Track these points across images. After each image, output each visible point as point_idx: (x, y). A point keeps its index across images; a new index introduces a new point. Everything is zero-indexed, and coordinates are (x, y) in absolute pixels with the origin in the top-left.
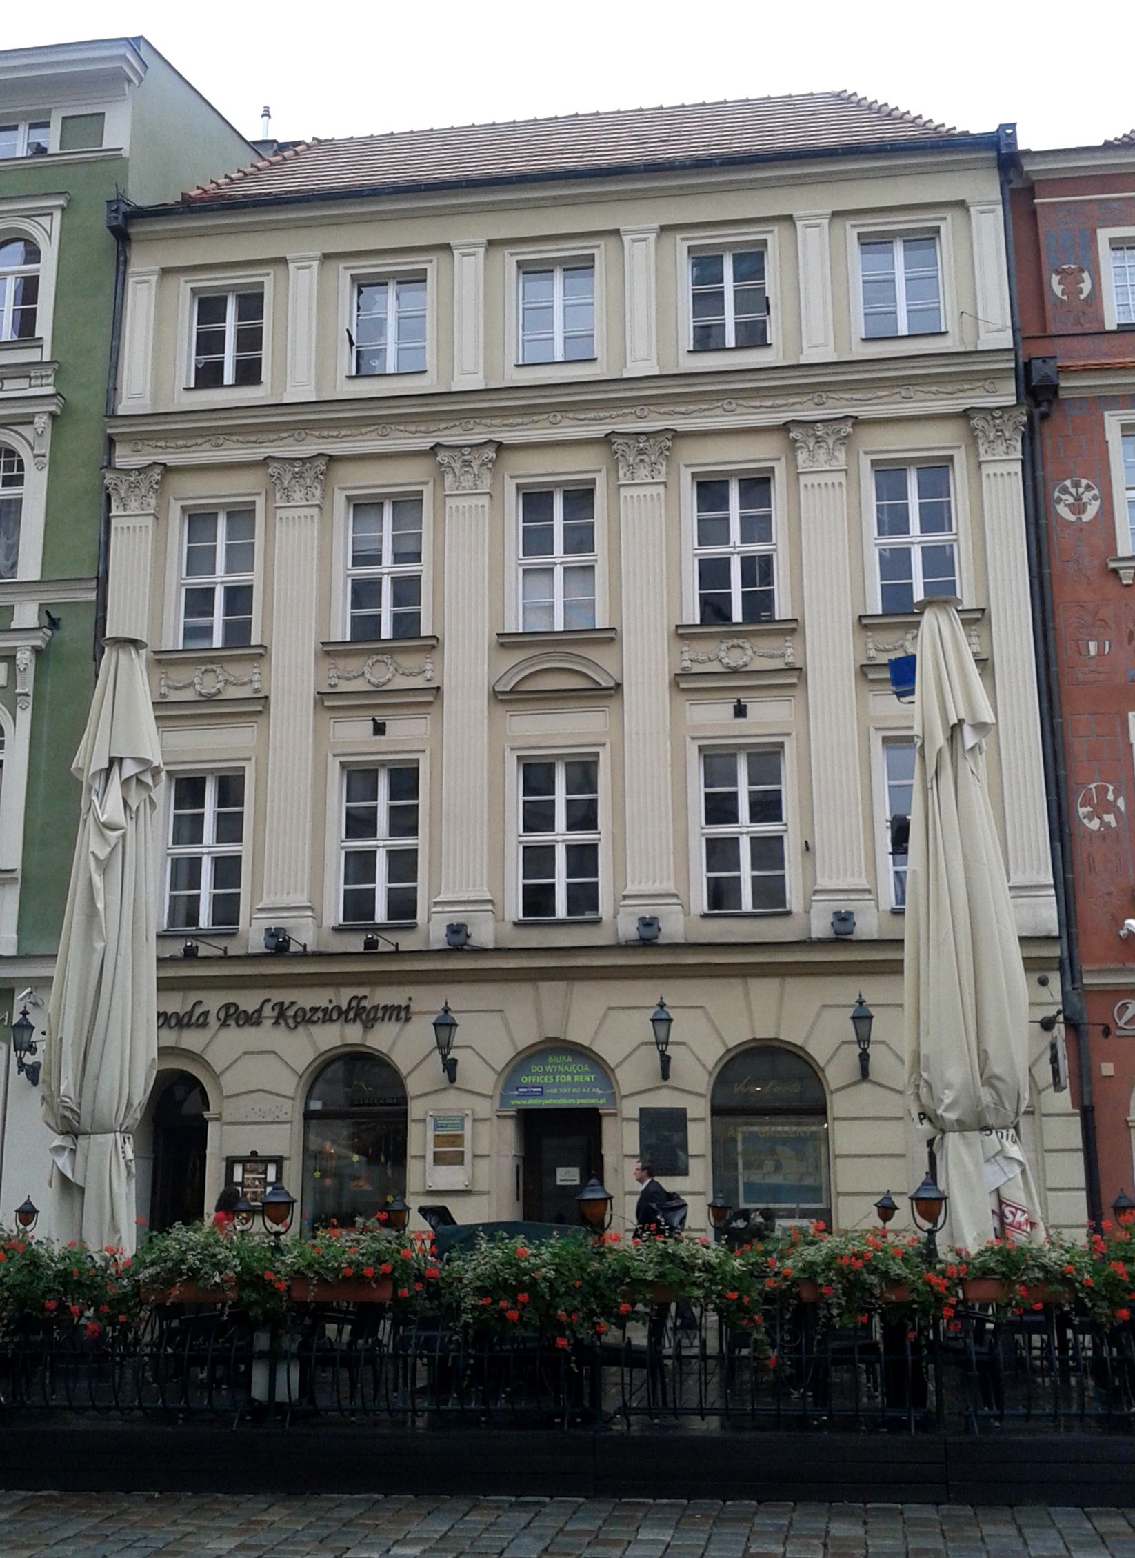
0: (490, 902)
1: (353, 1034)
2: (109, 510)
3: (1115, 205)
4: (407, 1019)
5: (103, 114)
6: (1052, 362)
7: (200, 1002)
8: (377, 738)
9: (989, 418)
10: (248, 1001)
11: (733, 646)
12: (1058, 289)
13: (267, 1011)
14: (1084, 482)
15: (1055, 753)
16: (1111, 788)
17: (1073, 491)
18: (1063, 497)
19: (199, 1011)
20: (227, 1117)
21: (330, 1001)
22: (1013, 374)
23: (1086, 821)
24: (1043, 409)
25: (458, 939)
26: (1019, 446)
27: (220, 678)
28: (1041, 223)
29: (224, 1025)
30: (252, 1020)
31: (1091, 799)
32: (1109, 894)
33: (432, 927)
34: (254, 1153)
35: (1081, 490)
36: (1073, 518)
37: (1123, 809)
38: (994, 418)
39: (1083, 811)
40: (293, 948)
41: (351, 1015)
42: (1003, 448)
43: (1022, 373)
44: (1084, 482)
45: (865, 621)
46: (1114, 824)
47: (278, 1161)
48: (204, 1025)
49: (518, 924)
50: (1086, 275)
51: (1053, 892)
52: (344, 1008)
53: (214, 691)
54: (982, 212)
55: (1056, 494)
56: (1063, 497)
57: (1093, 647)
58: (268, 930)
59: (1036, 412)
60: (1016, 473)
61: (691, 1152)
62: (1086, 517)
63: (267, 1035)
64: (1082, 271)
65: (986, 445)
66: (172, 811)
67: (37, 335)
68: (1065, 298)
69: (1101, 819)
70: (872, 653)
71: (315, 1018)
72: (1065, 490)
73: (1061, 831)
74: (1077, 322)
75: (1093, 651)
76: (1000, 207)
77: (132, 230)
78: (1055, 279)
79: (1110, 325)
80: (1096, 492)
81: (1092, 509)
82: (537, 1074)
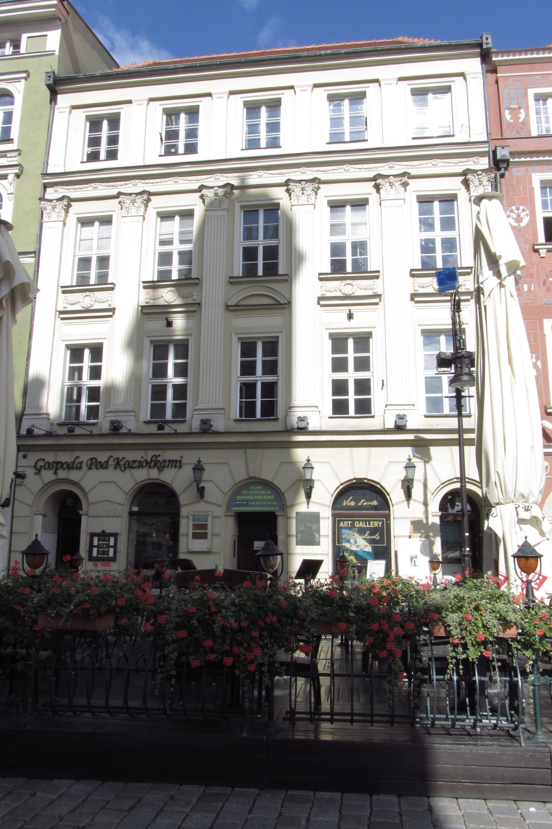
0: (223, 409)
1: (154, 474)
2: (42, 219)
3: (537, 77)
4: (180, 467)
5: (46, 36)
6: (507, 148)
7: (78, 457)
8: (168, 328)
10: (102, 457)
11: (348, 284)
13: (111, 462)
14: (521, 207)
17: (516, 212)
19: (78, 461)
20: (90, 514)
21: (142, 458)
24: (502, 171)
25: (206, 427)
27: (93, 299)
29: (90, 468)
30: (103, 466)
33: (194, 421)
34: (103, 531)
35: (520, 211)
38: (478, 175)
40: (123, 431)
41: (152, 464)
44: (521, 207)
45: (413, 273)
47: (115, 535)
48: (80, 468)
49: (236, 421)
50: (522, 111)
52: (149, 461)
53: (90, 305)
54: (473, 78)
56: (512, 215)
58: (111, 421)
59: (498, 173)
61: (321, 533)
62: (523, 224)
63: (111, 474)
64: (520, 108)
65: (474, 188)
66: (68, 365)
67: (11, 138)
68: (512, 121)
70: (417, 288)
71: (134, 466)
74: (518, 132)
76: (481, 76)
77: (58, 88)
78: (507, 112)
80: (527, 212)
81: (525, 221)
82: (245, 495)
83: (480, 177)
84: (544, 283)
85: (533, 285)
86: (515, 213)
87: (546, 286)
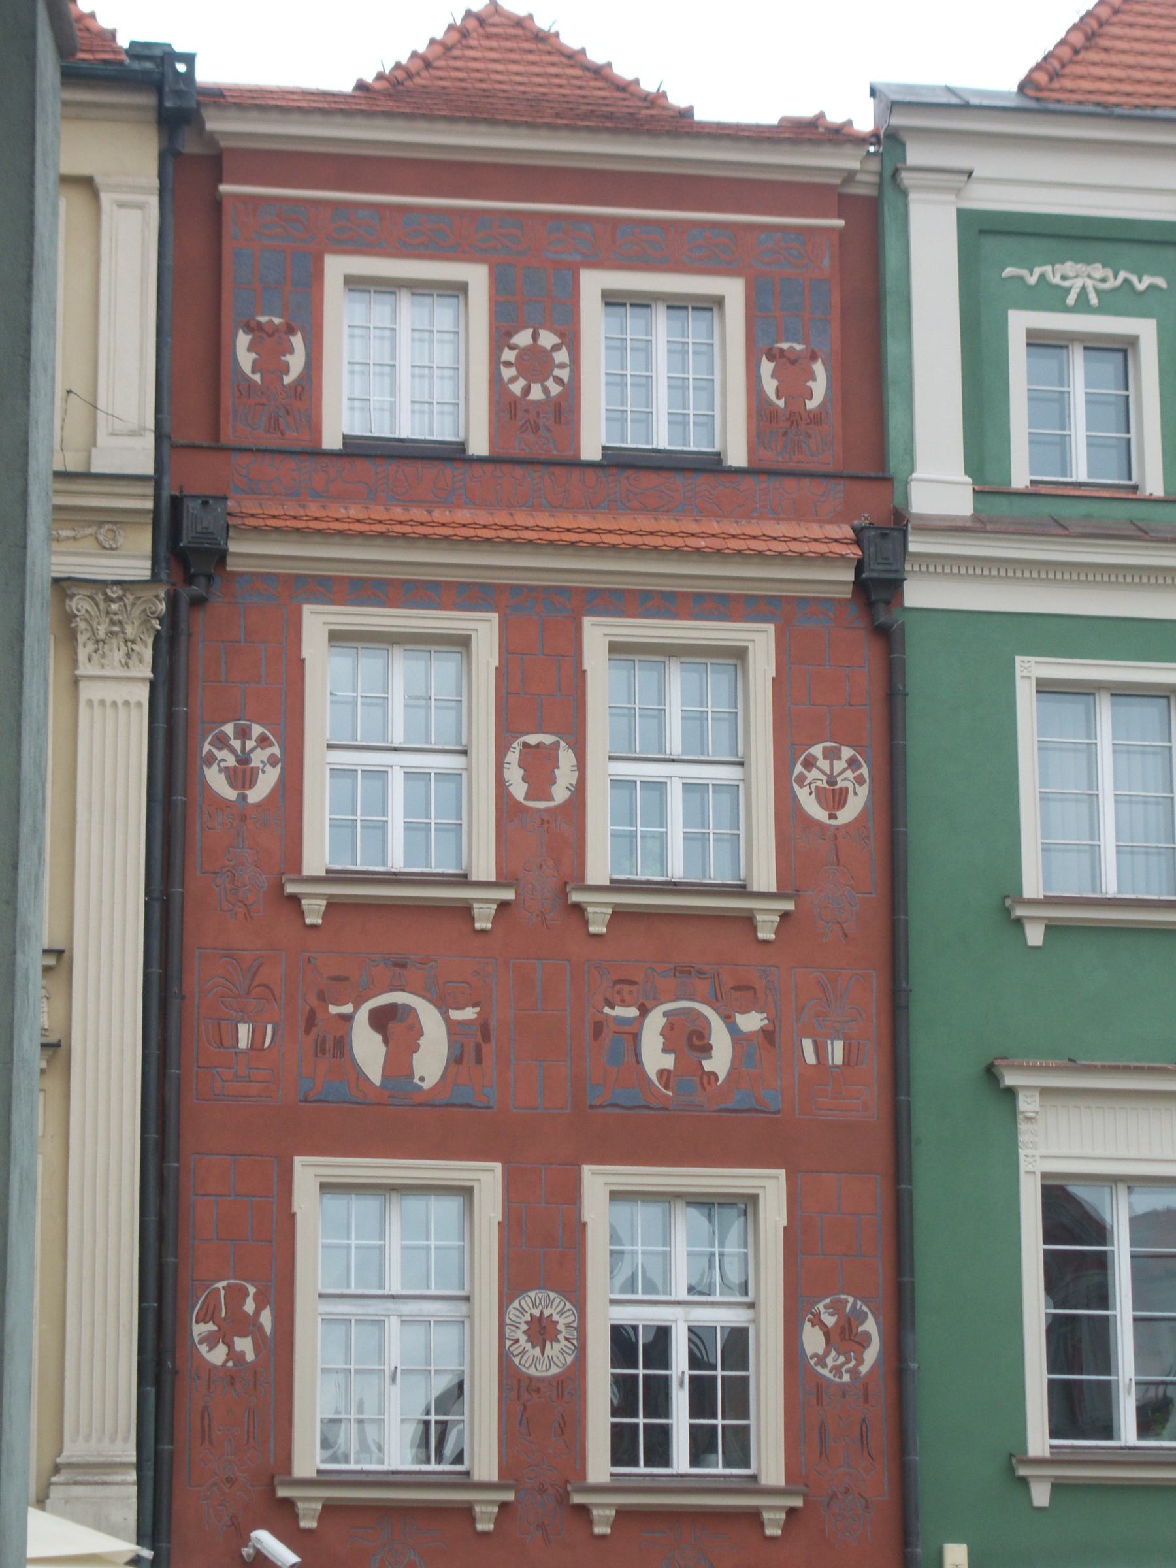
9: (100, 597)
12: (245, 359)
14: (257, 730)
15: (161, 1224)
16: (252, 1290)
17: (236, 744)
18: (220, 755)
22: (149, 519)
23: (203, 1349)
26: (148, 654)
28: (231, 228)
31: (217, 1308)
32: (230, 1481)
35: (250, 744)
36: (231, 794)
37: (268, 1327)
39: (200, 1329)
42: (119, 656)
44: (257, 730)
46: (250, 1356)
50: (297, 341)
51: (132, 1476)
54: (122, 205)
55: (207, 748)
56: (220, 755)
57: (244, 1031)
59: (185, 593)
60: (139, 704)
62: (256, 795)
64: (291, 330)
65: (91, 647)
68: (257, 378)
69: (230, 1346)
72: (222, 742)
73: (159, 1363)
74: (274, 425)
75: (243, 1044)
76: (154, 201)
78: (243, 340)
79: (331, 441)
81: (267, 782)
83: (114, 607)
84: (311, 1020)
85: (270, 1027)
86: (232, 751)
87: (315, 1031)
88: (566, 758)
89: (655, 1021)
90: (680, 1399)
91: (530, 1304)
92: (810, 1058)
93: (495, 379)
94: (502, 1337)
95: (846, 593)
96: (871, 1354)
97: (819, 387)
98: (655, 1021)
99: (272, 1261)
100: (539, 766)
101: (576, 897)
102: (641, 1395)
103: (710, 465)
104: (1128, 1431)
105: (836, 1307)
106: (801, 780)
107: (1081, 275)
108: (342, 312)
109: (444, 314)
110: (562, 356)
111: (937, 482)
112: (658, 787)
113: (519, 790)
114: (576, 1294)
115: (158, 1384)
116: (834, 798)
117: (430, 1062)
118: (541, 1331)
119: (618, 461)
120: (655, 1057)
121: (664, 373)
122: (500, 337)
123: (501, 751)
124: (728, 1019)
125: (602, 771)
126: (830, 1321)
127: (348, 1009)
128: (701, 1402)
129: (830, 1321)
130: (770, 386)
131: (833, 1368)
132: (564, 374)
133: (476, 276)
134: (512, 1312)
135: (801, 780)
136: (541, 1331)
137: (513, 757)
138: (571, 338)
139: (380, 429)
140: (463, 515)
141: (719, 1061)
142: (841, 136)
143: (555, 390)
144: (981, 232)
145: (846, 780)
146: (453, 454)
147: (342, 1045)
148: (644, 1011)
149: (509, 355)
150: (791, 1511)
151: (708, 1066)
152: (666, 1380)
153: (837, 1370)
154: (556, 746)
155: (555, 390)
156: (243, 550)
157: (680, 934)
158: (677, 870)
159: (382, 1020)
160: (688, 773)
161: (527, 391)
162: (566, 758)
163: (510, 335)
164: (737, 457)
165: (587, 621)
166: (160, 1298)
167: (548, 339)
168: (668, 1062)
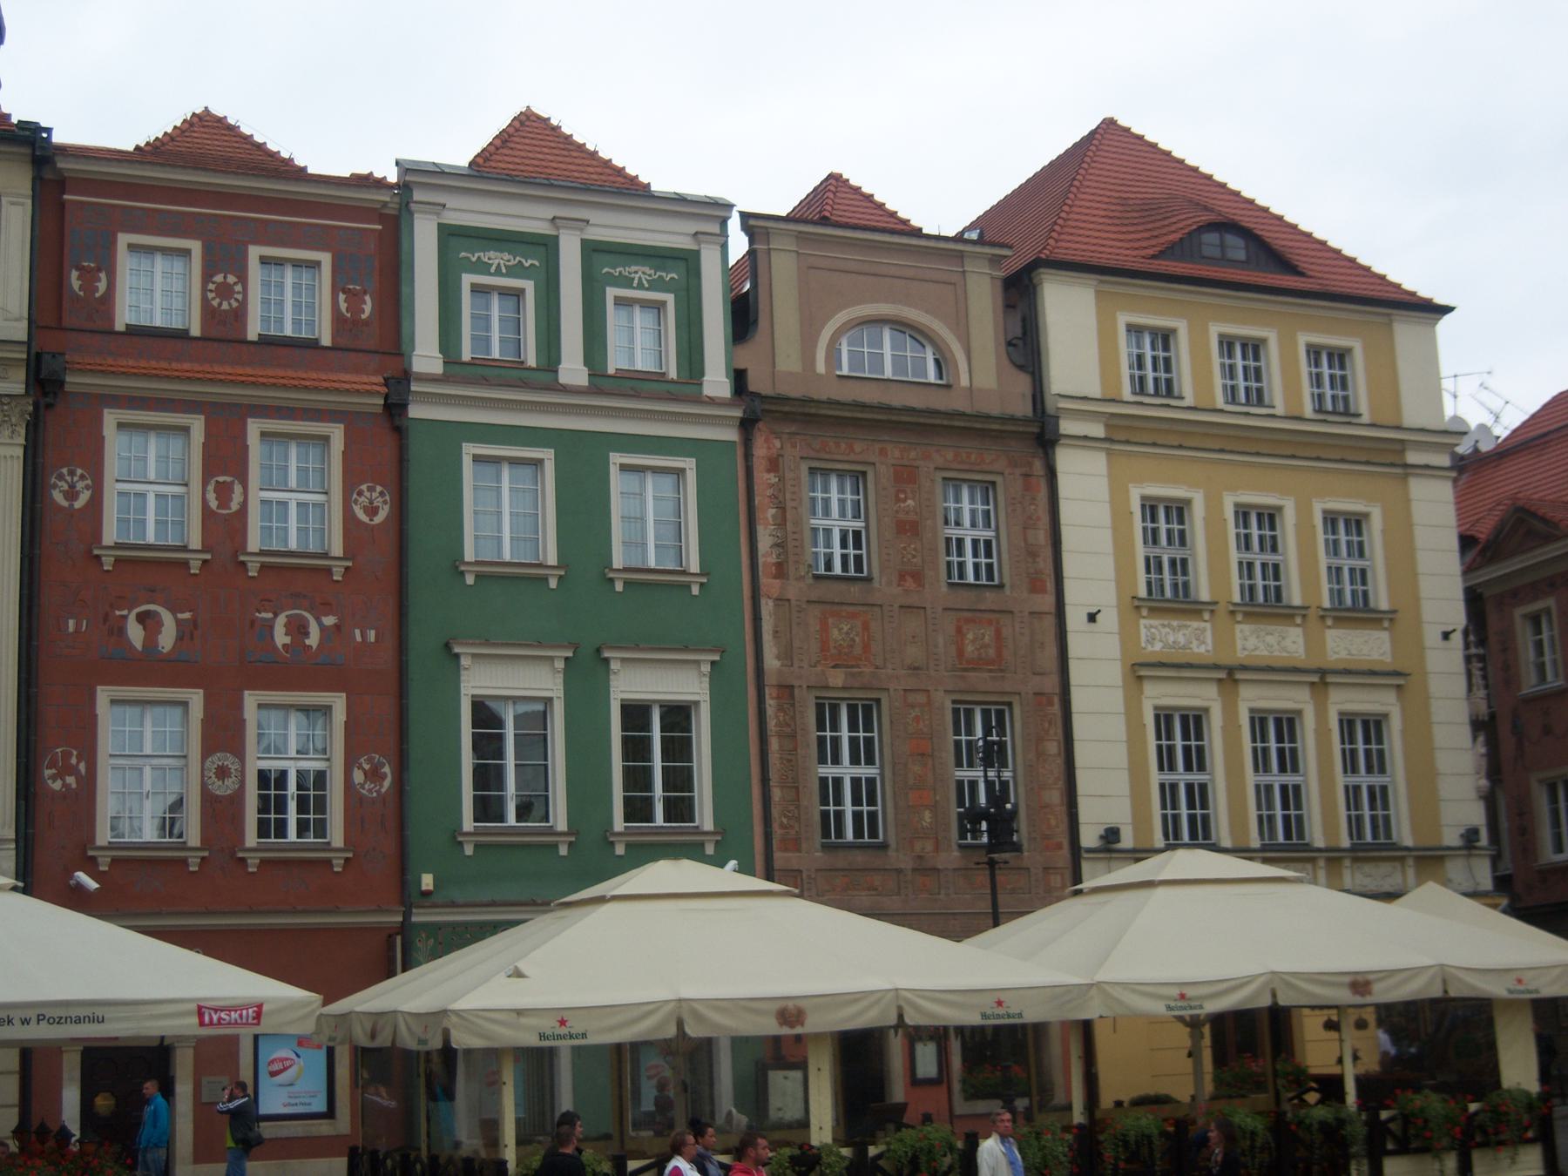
14: (79, 471)
26: (23, 432)
36: (65, 504)
39: (48, 772)
42: (7, 433)
43: (33, 364)
44: (79, 471)
50: (103, 275)
54: (12, 203)
57: (71, 623)
62: (78, 504)
64: (99, 270)
72: (61, 477)
75: (71, 629)
76: (29, 202)
78: (74, 274)
79: (119, 326)
81: (84, 497)
84: (106, 617)
88: (238, 488)
89: (281, 620)
90: (292, 806)
91: (217, 759)
92: (359, 639)
93: (205, 300)
94: (203, 776)
95: (380, 410)
96: (387, 783)
97: (368, 308)
98: (281, 620)
99: (85, 737)
100: (224, 492)
101: (242, 558)
102: (272, 804)
103: (313, 344)
104: (511, 819)
105: (370, 760)
106: (356, 502)
107: (496, 258)
108: (126, 263)
109: (178, 265)
110: (238, 288)
111: (426, 356)
112: (284, 504)
113: (213, 504)
114: (240, 754)
115: (26, 799)
116: (372, 511)
117: (167, 639)
118: (222, 773)
119: (266, 341)
120: (281, 638)
121: (290, 298)
122: (207, 277)
123: (205, 483)
124: (318, 619)
125: (256, 495)
126: (367, 767)
127: (125, 612)
128: (302, 806)
129: (367, 767)
130: (343, 306)
131: (368, 790)
132: (240, 297)
133: (195, 246)
134: (208, 764)
135: (356, 502)
136: (222, 773)
137: (211, 488)
138: (243, 279)
139: (144, 321)
140: (186, 366)
141: (313, 640)
142: (380, 184)
143: (235, 304)
144: (450, 235)
145: (378, 502)
146: (182, 335)
147: (121, 631)
148: (276, 615)
149: (211, 286)
150: (347, 860)
151: (307, 642)
152: (285, 796)
153: (370, 791)
154: (232, 483)
155: (235, 304)
156: (73, 381)
157: (295, 577)
158: (293, 545)
159: (142, 618)
160: (298, 499)
161: (220, 304)
162: (238, 488)
163: (212, 276)
164: (326, 341)
165: (250, 420)
166: (27, 757)
167: (231, 279)
168: (288, 640)
